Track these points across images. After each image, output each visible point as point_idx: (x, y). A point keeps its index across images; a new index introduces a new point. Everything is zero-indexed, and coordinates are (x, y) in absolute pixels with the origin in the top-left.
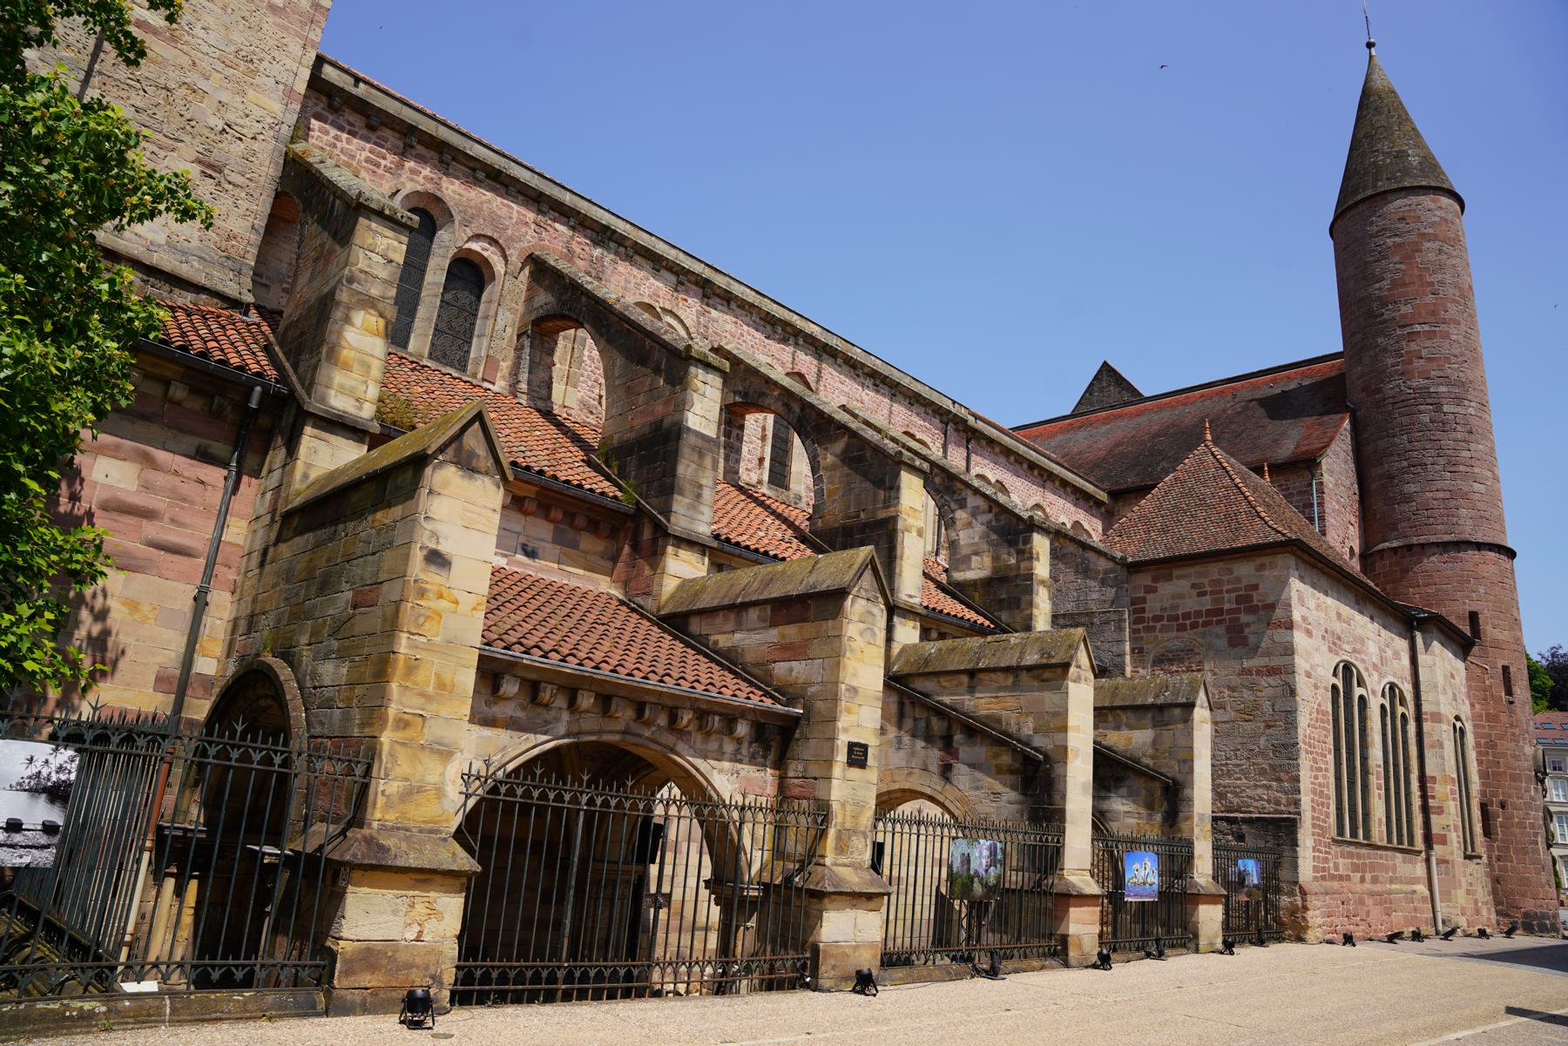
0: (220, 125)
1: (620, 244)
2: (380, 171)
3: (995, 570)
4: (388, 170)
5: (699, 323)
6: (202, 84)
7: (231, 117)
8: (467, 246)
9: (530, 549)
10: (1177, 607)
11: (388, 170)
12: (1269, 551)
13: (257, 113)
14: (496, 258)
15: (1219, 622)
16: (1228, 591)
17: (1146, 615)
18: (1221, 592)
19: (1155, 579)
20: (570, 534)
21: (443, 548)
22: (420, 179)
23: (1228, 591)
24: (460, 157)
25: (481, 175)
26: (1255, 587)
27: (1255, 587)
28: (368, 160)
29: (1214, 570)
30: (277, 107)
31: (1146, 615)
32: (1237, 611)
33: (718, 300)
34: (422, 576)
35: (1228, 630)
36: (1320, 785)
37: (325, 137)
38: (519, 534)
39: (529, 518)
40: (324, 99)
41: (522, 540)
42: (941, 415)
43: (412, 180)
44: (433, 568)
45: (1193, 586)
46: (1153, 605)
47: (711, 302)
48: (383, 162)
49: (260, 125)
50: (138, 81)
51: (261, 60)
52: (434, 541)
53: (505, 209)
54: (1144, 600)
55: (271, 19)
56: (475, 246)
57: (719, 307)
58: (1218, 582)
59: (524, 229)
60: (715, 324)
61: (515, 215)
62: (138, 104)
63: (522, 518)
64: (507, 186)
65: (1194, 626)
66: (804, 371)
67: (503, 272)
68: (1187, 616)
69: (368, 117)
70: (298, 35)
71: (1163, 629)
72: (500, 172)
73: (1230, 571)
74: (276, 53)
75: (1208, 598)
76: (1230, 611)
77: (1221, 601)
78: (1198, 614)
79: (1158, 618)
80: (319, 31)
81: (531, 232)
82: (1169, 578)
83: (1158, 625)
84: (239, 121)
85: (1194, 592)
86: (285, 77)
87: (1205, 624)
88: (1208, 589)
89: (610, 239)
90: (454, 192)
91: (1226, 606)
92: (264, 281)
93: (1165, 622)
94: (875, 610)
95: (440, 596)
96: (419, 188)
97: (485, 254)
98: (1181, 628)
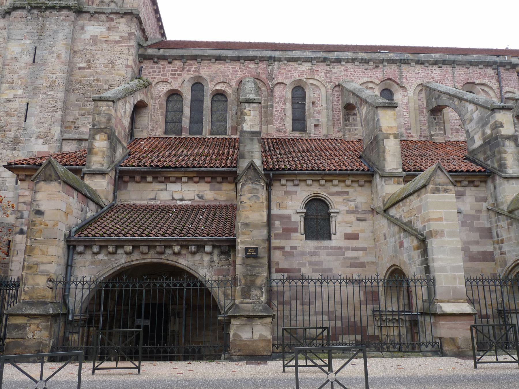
0: (107, 87)
1: (280, 61)
2: (177, 76)
3: (484, 140)
4: (179, 74)
5: (327, 77)
6: (99, 78)
7: (110, 83)
8: (215, 89)
9: (200, 195)
11: (179, 74)
13: (118, 77)
14: (227, 89)
20: (218, 185)
21: (42, 208)
22: (192, 72)
24: (204, 58)
25: (214, 61)
28: (171, 74)
30: (124, 73)
33: (335, 64)
34: (34, 219)
37: (155, 73)
38: (195, 191)
39: (198, 184)
40: (152, 61)
41: (197, 193)
42: (491, 66)
43: (188, 74)
44: (37, 216)
47: (331, 66)
48: (177, 73)
49: (120, 82)
50: (82, 85)
51: (116, 61)
52: (37, 207)
53: (226, 69)
55: (117, 45)
56: (218, 87)
57: (336, 67)
61: (231, 69)
62: (83, 92)
63: (195, 185)
64: (225, 60)
66: (391, 77)
67: (231, 93)
69: (167, 60)
70: (126, 46)
72: (220, 56)
74: (120, 56)
80: (132, 41)
84: (113, 83)
86: (124, 62)
89: (275, 61)
90: (205, 71)
92: (140, 130)
94: (258, 187)
95: (41, 224)
96: (192, 76)
97: (223, 89)
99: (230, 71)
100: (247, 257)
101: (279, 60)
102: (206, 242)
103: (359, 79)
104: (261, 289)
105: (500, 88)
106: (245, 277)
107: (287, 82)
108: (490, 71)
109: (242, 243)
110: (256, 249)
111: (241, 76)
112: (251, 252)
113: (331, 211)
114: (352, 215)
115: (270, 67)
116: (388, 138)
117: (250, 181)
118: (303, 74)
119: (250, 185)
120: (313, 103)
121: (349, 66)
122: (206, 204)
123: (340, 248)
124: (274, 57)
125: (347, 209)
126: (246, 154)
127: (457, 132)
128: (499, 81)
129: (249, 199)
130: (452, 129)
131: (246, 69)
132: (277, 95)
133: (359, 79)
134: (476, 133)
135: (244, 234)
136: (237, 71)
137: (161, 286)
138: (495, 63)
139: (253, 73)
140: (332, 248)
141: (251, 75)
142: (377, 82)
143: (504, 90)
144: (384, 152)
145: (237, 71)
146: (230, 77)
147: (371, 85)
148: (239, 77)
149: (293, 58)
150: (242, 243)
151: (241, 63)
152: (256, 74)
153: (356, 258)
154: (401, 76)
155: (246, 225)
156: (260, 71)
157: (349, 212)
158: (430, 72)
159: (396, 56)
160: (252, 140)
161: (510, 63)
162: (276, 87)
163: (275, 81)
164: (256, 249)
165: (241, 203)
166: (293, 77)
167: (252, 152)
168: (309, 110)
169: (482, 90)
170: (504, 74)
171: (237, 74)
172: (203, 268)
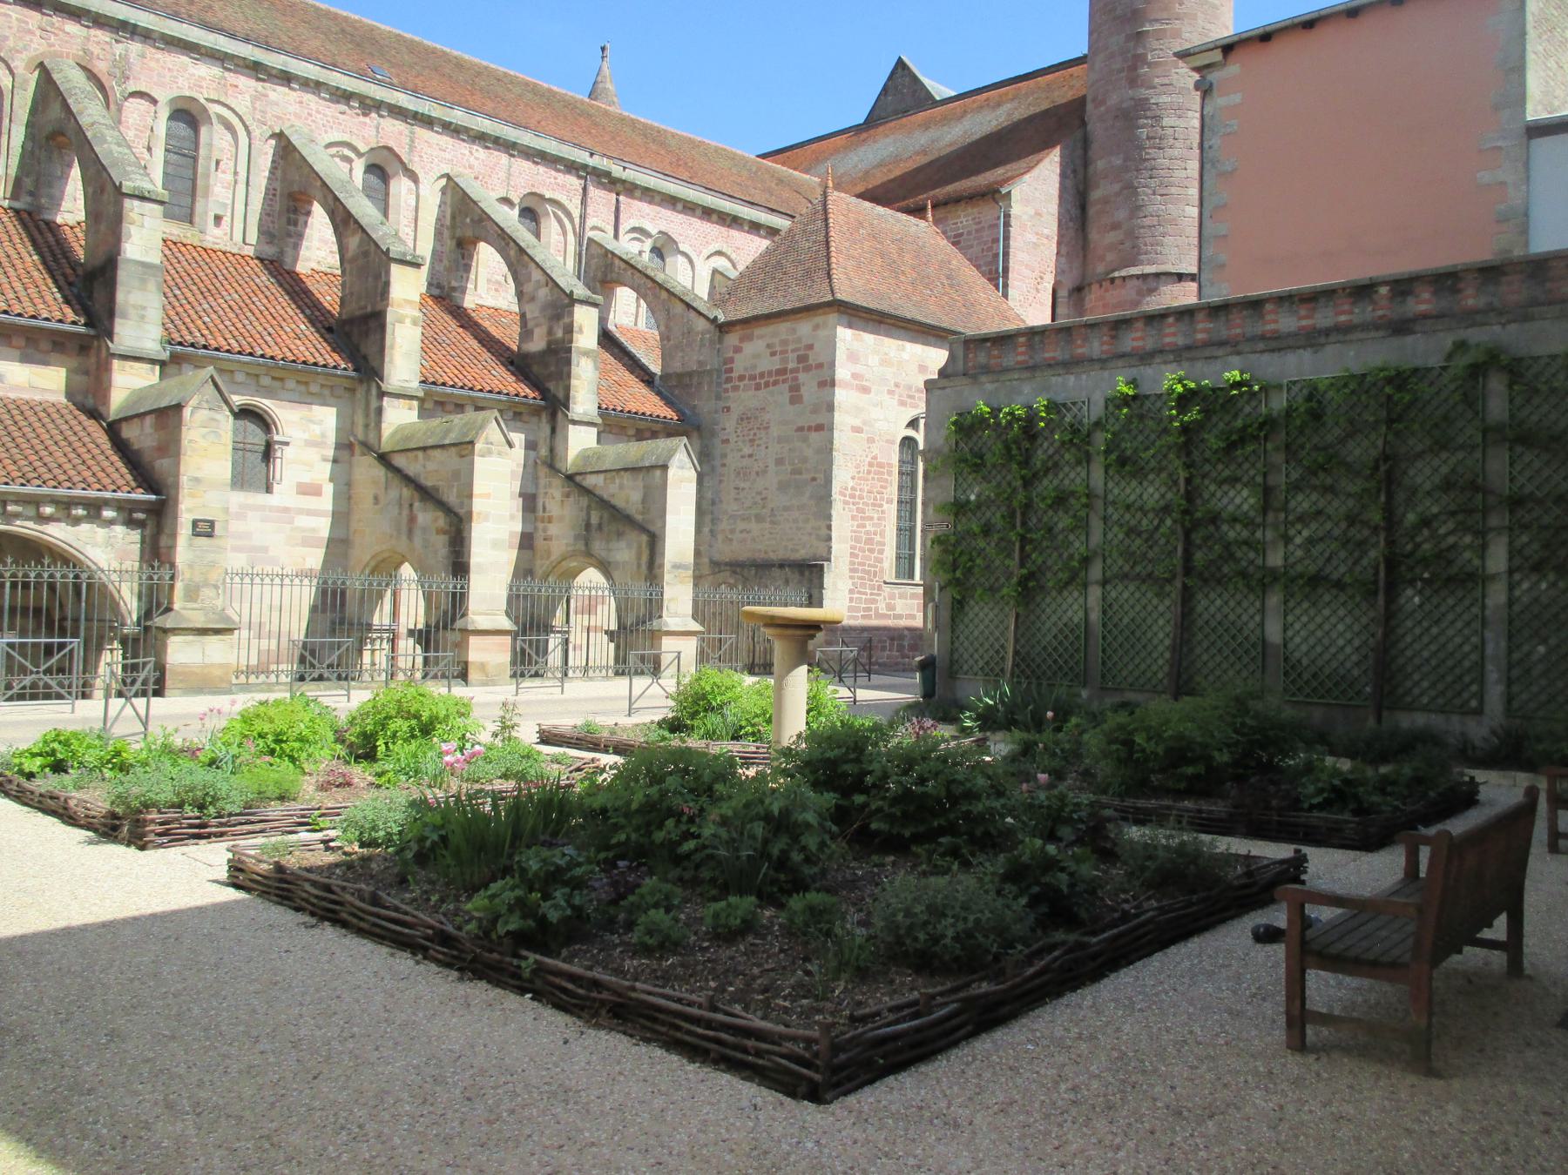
5: (255, 109)
10: (755, 367)
12: (821, 311)
15: (784, 381)
16: (793, 351)
17: (733, 375)
18: (786, 352)
19: (742, 340)
23: (793, 351)
26: (810, 347)
27: (810, 347)
29: (783, 328)
31: (733, 375)
32: (796, 370)
35: (792, 389)
36: (867, 533)
42: (577, 170)
45: (768, 346)
46: (740, 365)
54: (731, 360)
58: (784, 342)
59: (28, 38)
60: (275, 108)
61: (15, 23)
65: (767, 385)
66: (391, 144)
68: (762, 375)
71: (746, 388)
73: (794, 331)
75: (777, 358)
76: (793, 371)
77: (784, 360)
78: (770, 373)
79: (741, 378)
81: (36, 39)
82: (749, 338)
83: (742, 384)
85: (769, 351)
87: (775, 383)
88: (778, 348)
91: (791, 366)
93: (746, 382)
98: (758, 387)
99: (10, 28)
100: (196, 534)
101: (145, 35)
102: (106, 503)
103: (326, 132)
104: (216, 587)
105: (583, 217)
106: (191, 566)
107: (163, 96)
108: (574, 182)
109: (189, 510)
110: (212, 524)
111: (41, 50)
112: (203, 527)
113: (276, 438)
114: (316, 449)
115: (120, 46)
116: (401, 322)
117: (205, 405)
118: (201, 87)
119: (206, 412)
120: (218, 163)
121: (309, 98)
122: (13, 395)
123: (286, 510)
124: (135, 26)
125: (306, 436)
126: (132, 312)
127: (496, 290)
128: (584, 202)
129: (204, 437)
130: (489, 281)
131: (56, 35)
132: (131, 121)
133: (326, 132)
134: (537, 325)
135: (192, 496)
136: (30, 32)
137: (39, 575)
138: (585, 167)
139: (75, 50)
140: (272, 509)
141: (68, 54)
142: (363, 148)
143: (590, 223)
144: (392, 347)
145: (30, 32)
146: (11, 43)
147: (347, 152)
148: (36, 49)
149: (180, 40)
150: (189, 510)
151: (44, 14)
152: (81, 53)
153: (313, 530)
154: (412, 147)
155: (197, 480)
156: (96, 50)
157: (310, 443)
158: (467, 152)
159: (409, 101)
160: (143, 281)
161: (608, 174)
162: (131, 100)
163: (132, 87)
164: (212, 524)
165: (190, 441)
166: (175, 86)
167: (144, 308)
168: (208, 176)
169: (554, 213)
170: (594, 192)
171: (31, 41)
172: (95, 545)
